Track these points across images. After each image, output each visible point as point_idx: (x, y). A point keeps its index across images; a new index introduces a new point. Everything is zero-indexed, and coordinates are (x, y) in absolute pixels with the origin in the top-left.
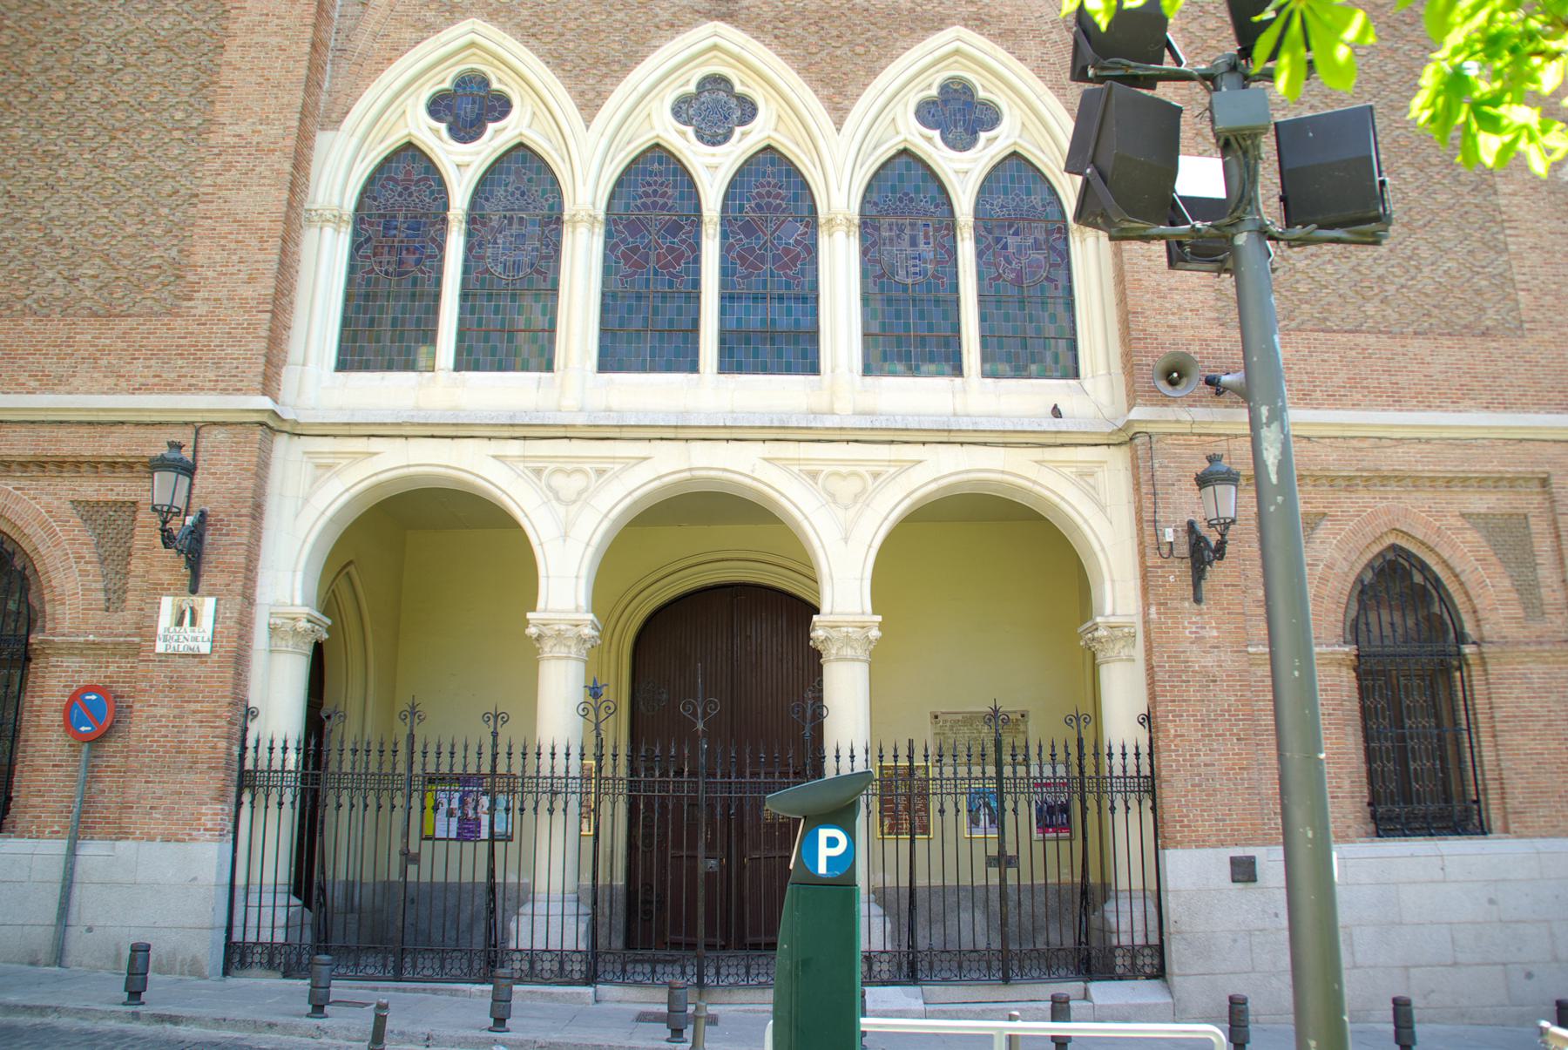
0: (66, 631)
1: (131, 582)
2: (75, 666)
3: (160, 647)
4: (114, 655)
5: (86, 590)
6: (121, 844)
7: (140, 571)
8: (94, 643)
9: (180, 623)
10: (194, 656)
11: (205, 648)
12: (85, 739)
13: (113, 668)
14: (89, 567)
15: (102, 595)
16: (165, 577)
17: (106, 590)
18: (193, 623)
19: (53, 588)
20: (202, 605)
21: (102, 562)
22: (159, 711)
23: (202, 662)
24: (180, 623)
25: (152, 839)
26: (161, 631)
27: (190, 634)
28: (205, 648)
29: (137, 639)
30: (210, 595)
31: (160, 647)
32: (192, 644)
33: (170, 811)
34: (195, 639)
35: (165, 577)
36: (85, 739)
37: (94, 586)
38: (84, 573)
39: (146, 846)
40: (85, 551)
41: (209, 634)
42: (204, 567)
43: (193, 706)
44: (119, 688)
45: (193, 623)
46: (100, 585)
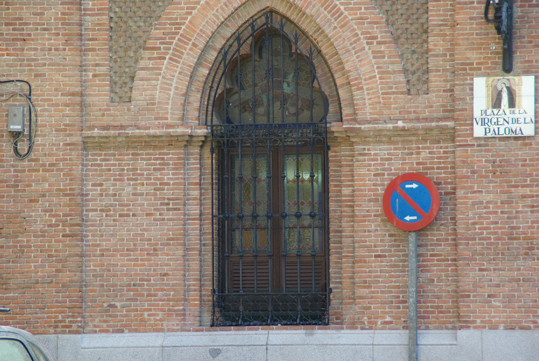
0: (369, 117)
1: (432, 63)
2: (384, 154)
3: (479, 131)
4: (425, 140)
5: (383, 73)
6: (462, 334)
7: (440, 50)
8: (403, 129)
9: (497, 104)
10: (516, 138)
11: (529, 130)
12: (408, 228)
13: (425, 154)
14: (383, 48)
15: (401, 78)
16: (473, 56)
17: (405, 71)
18: (512, 104)
19: (345, 73)
20: (520, 84)
21: (396, 39)
22: (485, 197)
23: (526, 145)
24: (497, 104)
25: (494, 327)
26: (477, 114)
27: (509, 116)
28: (529, 130)
29: (450, 124)
30: (527, 72)
31: (479, 131)
32: (514, 127)
33: (509, 299)
34: (517, 121)
35: (473, 56)
36: (408, 228)
37: (391, 68)
38: (378, 55)
39: (489, 335)
40: (376, 31)
41: (531, 114)
42: (517, 43)
43: (521, 191)
44: (435, 175)
45: (512, 104)
46: (398, 67)
